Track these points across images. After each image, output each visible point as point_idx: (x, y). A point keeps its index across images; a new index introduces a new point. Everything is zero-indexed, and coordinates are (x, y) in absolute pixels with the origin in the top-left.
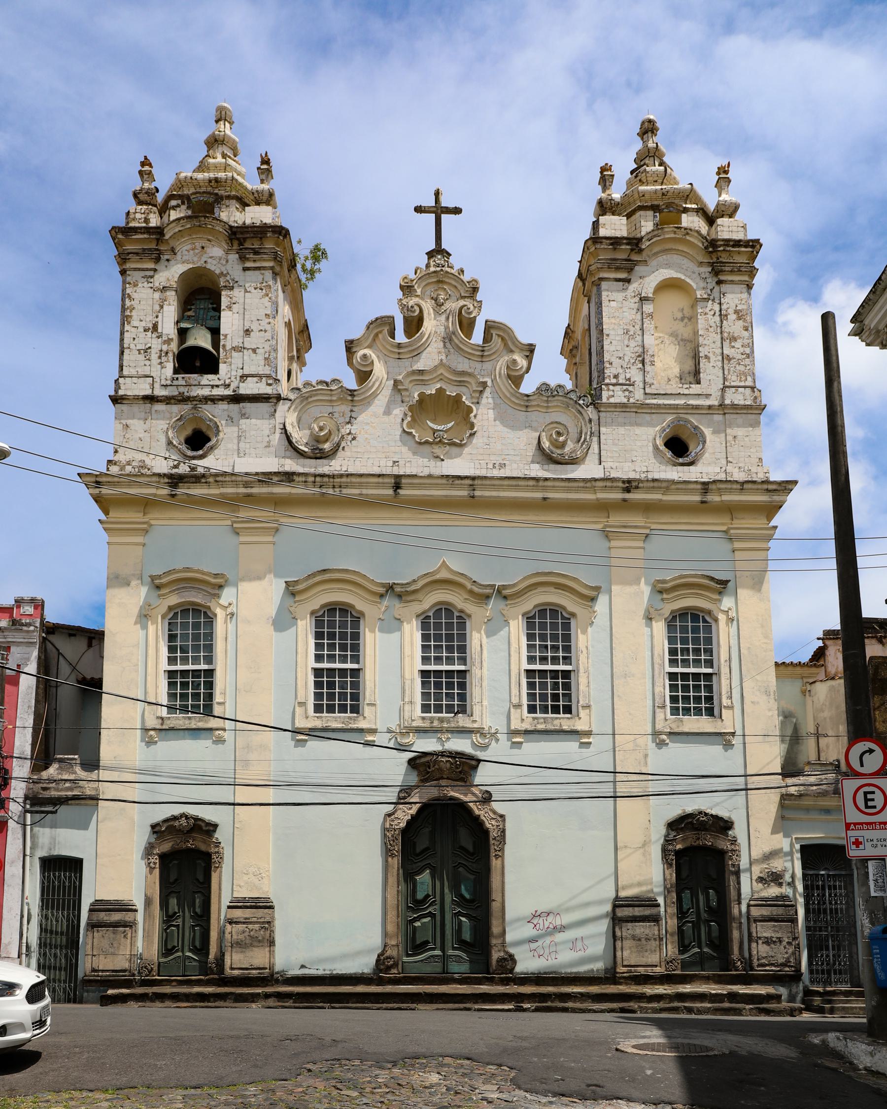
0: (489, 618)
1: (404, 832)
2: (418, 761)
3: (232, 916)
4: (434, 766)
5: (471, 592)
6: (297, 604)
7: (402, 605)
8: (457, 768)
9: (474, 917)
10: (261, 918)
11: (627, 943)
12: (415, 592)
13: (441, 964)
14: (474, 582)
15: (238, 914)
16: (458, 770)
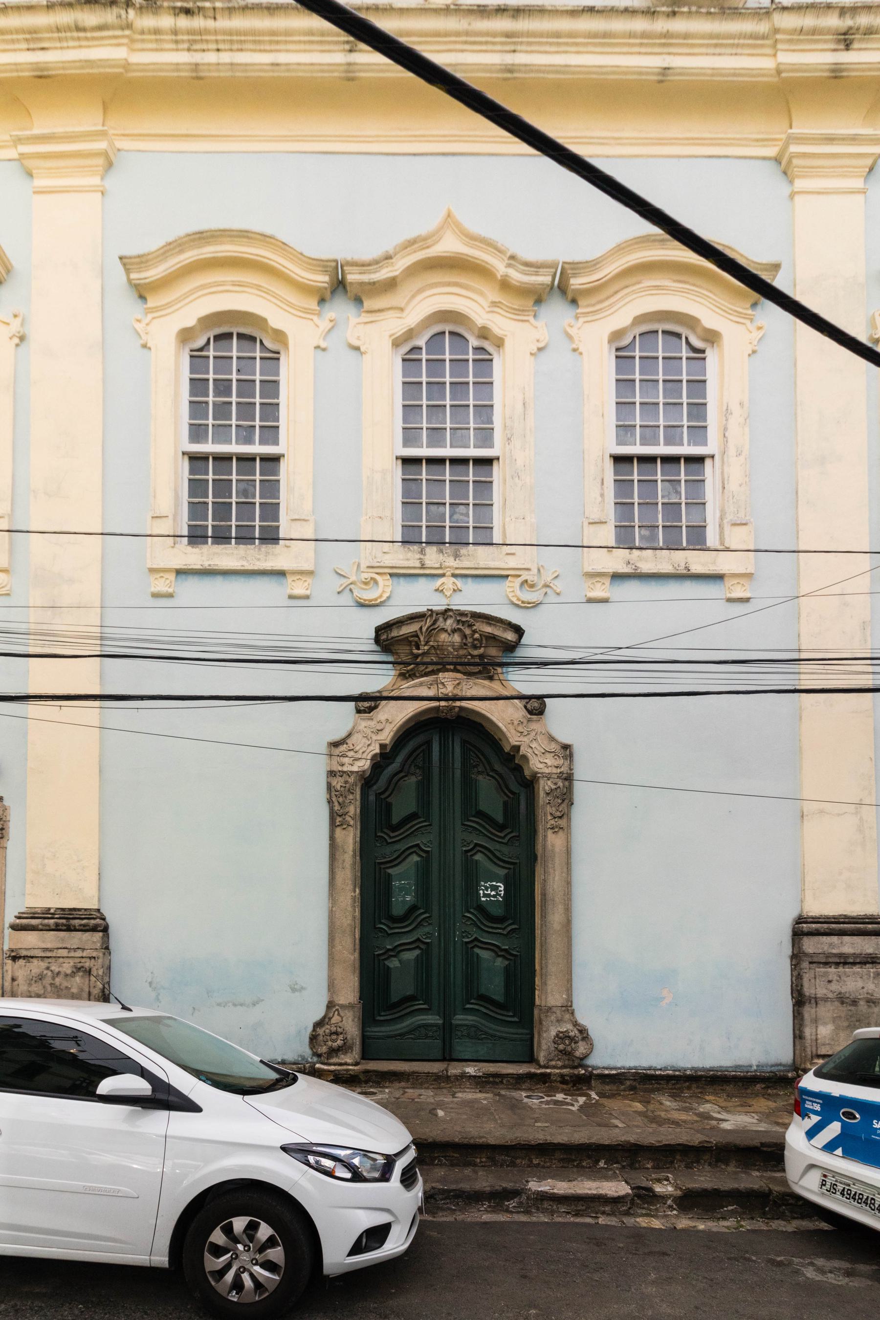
0: (541, 345)
1: (368, 781)
2: (395, 633)
3: (19, 946)
4: (426, 643)
5: (505, 285)
6: (150, 316)
7: (365, 317)
8: (475, 647)
9: (505, 950)
10: (75, 950)
11: (825, 1011)
12: (391, 285)
13: (438, 1042)
14: (512, 257)
15: (30, 940)
16: (476, 652)
